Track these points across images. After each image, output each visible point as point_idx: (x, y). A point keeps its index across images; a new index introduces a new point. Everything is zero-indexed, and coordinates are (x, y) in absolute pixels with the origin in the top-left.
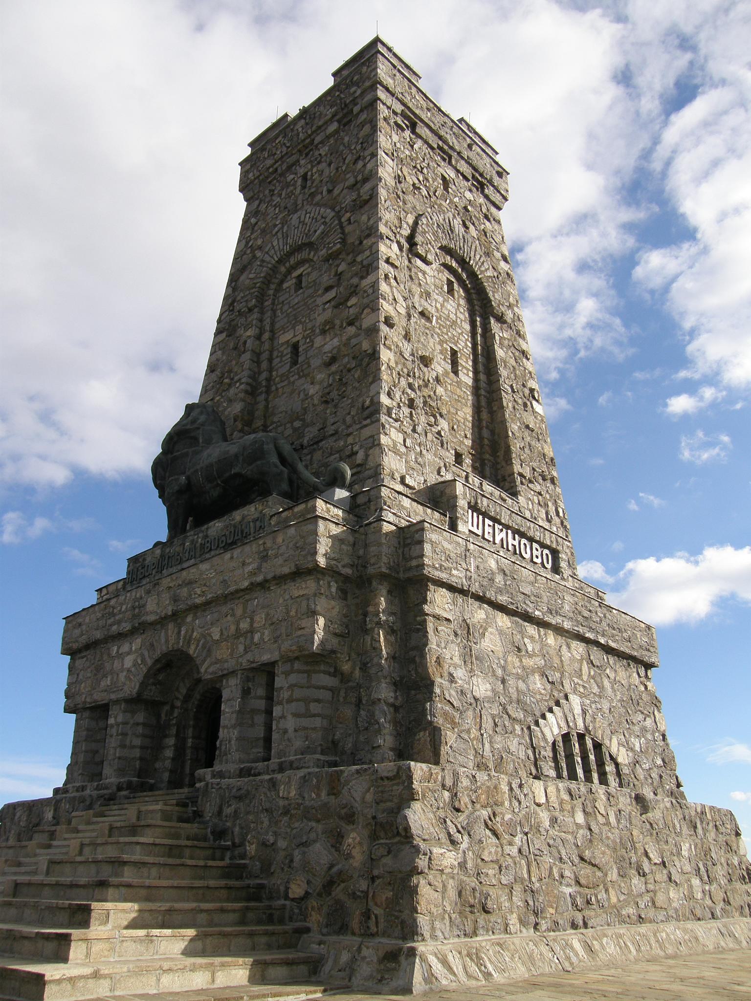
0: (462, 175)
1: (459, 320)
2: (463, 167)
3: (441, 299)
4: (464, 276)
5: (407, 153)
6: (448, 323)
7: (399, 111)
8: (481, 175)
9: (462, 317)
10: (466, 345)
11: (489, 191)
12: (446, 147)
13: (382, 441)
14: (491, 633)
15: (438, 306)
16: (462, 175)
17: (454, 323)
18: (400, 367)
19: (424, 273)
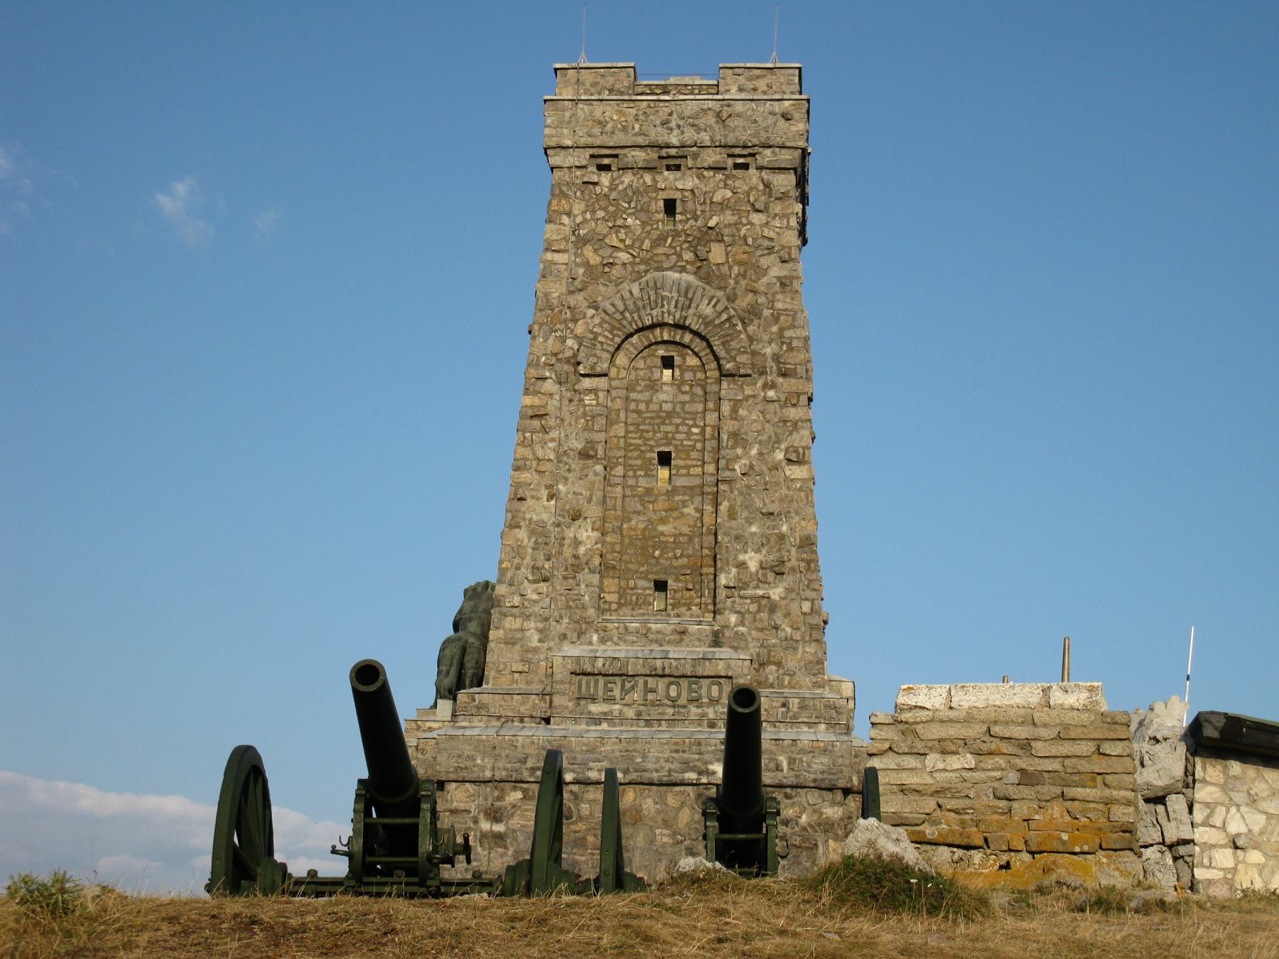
0: (710, 168)
1: (678, 409)
2: (711, 157)
3: (647, 395)
4: (687, 338)
5: (601, 214)
6: (657, 421)
7: (584, 163)
8: (745, 147)
9: (686, 398)
10: (689, 434)
11: (767, 156)
12: (673, 152)
13: (491, 637)
14: (526, 810)
15: (642, 407)
16: (710, 168)
17: (670, 414)
18: (533, 540)
19: (594, 391)
